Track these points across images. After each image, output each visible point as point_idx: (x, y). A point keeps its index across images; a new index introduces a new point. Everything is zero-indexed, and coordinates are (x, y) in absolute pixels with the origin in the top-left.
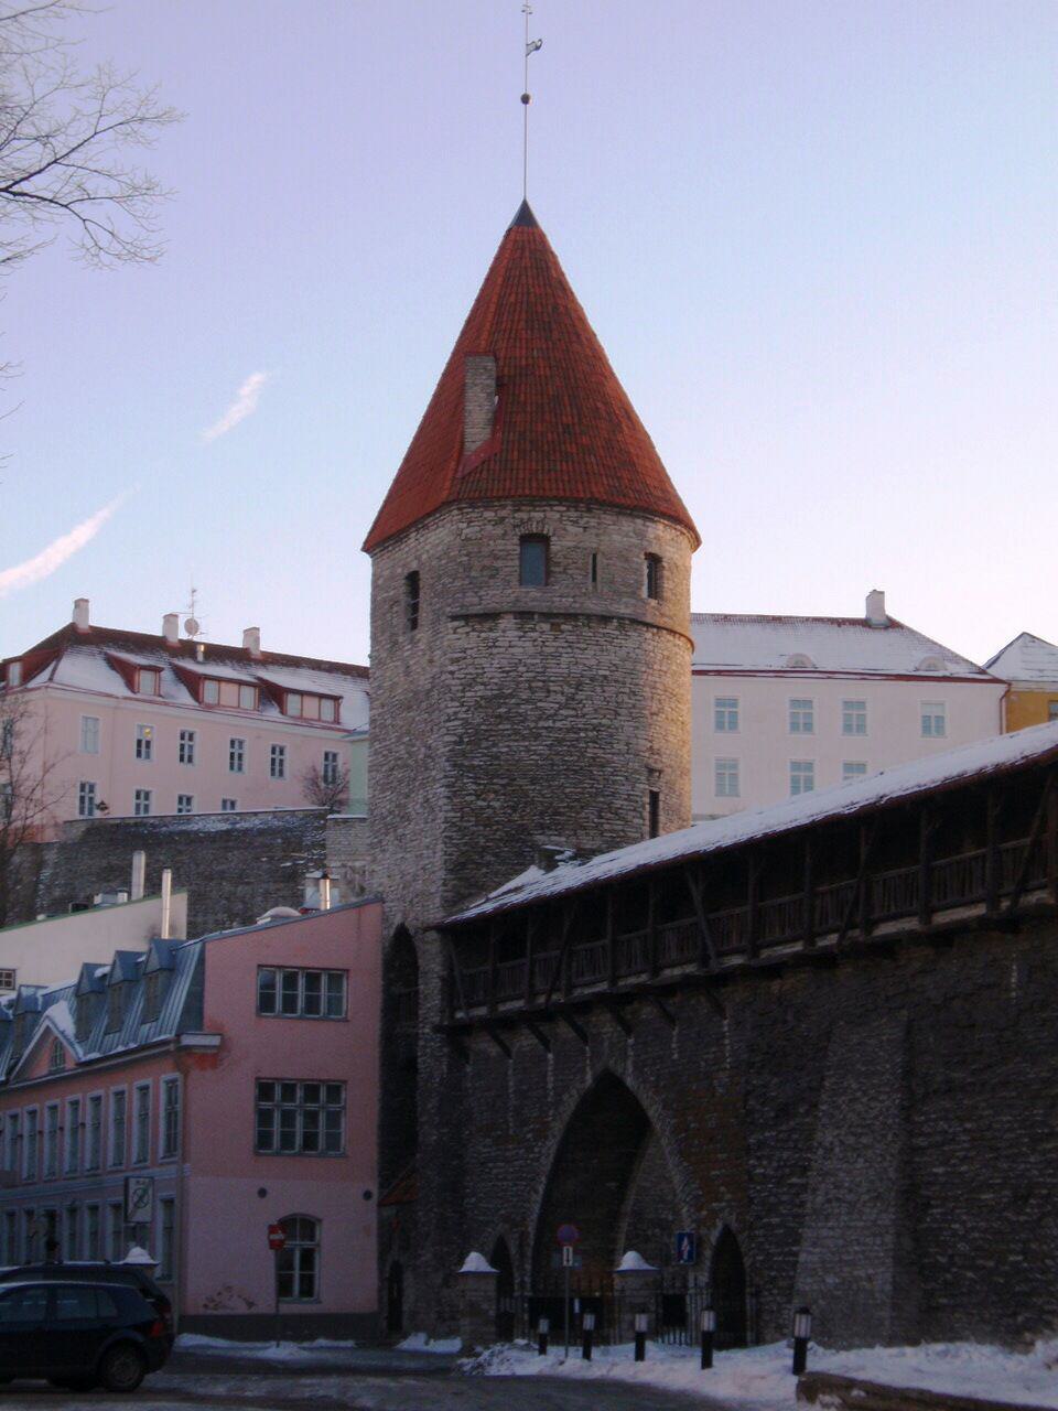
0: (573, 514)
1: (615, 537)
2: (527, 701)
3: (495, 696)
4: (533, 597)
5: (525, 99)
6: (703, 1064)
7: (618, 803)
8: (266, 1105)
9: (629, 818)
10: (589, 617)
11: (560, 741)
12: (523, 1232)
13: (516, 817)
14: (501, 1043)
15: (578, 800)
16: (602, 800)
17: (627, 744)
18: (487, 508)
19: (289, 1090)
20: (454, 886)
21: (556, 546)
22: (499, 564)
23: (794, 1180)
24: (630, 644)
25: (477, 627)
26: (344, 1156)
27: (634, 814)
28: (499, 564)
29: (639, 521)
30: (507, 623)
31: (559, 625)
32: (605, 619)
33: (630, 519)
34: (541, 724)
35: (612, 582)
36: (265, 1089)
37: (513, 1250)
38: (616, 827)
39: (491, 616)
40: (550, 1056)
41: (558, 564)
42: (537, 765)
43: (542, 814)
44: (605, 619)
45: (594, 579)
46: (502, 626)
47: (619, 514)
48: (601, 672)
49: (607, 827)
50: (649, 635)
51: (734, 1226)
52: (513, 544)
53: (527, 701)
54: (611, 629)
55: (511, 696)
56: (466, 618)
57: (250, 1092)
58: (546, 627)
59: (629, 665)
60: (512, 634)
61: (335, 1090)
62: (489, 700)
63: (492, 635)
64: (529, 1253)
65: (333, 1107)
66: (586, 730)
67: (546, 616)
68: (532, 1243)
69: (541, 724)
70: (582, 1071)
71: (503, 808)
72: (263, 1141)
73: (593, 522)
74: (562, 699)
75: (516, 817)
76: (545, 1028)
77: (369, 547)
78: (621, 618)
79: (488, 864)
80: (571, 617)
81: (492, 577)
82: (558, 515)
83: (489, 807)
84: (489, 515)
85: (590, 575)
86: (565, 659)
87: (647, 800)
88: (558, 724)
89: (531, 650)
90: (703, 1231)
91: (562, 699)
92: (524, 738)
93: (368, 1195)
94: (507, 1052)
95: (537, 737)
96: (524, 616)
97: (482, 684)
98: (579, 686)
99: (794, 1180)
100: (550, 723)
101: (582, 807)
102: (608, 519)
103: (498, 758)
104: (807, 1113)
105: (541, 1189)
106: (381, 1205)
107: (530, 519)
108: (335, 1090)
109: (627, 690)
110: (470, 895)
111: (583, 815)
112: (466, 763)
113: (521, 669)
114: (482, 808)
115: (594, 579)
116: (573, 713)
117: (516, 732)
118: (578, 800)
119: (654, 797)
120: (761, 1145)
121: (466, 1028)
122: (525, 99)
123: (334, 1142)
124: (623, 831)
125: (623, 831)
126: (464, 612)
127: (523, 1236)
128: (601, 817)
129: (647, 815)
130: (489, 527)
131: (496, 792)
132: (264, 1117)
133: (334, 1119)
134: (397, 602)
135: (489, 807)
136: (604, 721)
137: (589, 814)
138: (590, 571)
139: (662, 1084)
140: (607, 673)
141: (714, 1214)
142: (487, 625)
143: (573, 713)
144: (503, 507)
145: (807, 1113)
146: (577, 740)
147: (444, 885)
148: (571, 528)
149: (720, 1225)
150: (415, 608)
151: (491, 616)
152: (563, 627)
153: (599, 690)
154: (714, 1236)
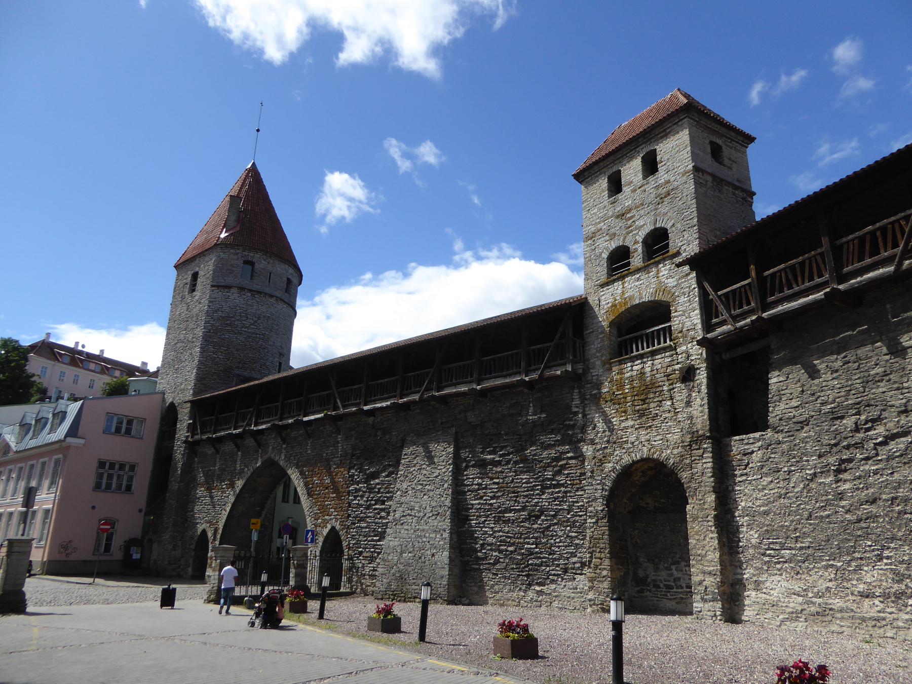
1: (278, 269)
2: (238, 320)
3: (226, 317)
4: (246, 283)
5: (258, 130)
6: (325, 455)
8: (101, 471)
10: (266, 294)
11: (249, 337)
12: (216, 528)
13: (228, 362)
14: (216, 449)
15: (253, 360)
18: (232, 248)
19: (112, 466)
20: (199, 387)
21: (257, 266)
22: (234, 269)
23: (377, 506)
25: (222, 290)
26: (133, 493)
28: (234, 269)
29: (287, 266)
30: (234, 290)
32: (271, 296)
36: (102, 464)
37: (210, 535)
39: (229, 287)
40: (239, 453)
41: (257, 273)
42: (239, 344)
43: (239, 363)
45: (269, 282)
46: (232, 292)
50: (285, 306)
51: (338, 527)
52: (240, 262)
53: (238, 320)
54: (273, 300)
55: (232, 317)
56: (218, 287)
57: (95, 464)
58: (249, 294)
60: (236, 295)
61: (132, 467)
62: (224, 317)
63: (228, 294)
64: (219, 536)
65: (131, 474)
66: (260, 334)
67: (250, 291)
68: (221, 532)
70: (257, 460)
71: (223, 358)
72: (98, 486)
73: (271, 261)
74: (252, 322)
75: (228, 362)
76: (239, 441)
77: (176, 267)
79: (215, 379)
80: (259, 293)
81: (230, 273)
82: (259, 256)
83: (218, 357)
84: (232, 251)
86: (255, 307)
87: (278, 364)
88: (249, 331)
89: (243, 302)
90: (318, 529)
91: (252, 322)
92: (236, 334)
93: (140, 511)
94: (217, 452)
95: (241, 334)
96: (242, 289)
97: (222, 311)
98: (259, 318)
99: (377, 506)
100: (246, 330)
103: (224, 340)
104: (387, 476)
105: (228, 509)
106: (145, 515)
107: (248, 255)
108: (132, 467)
110: (205, 390)
111: (254, 365)
112: (211, 340)
114: (215, 357)
115: (269, 282)
117: (232, 331)
118: (253, 360)
119: (280, 364)
120: (357, 490)
121: (198, 443)
123: (129, 488)
126: (217, 284)
127: (216, 530)
130: (232, 256)
131: (221, 352)
132: (100, 476)
133: (131, 479)
134: (186, 284)
135: (218, 357)
136: (267, 333)
139: (300, 464)
141: (326, 522)
142: (226, 290)
144: (239, 249)
145: (387, 476)
146: (256, 337)
147: (195, 386)
149: (329, 526)
150: (195, 285)
151: (229, 287)
154: (325, 531)
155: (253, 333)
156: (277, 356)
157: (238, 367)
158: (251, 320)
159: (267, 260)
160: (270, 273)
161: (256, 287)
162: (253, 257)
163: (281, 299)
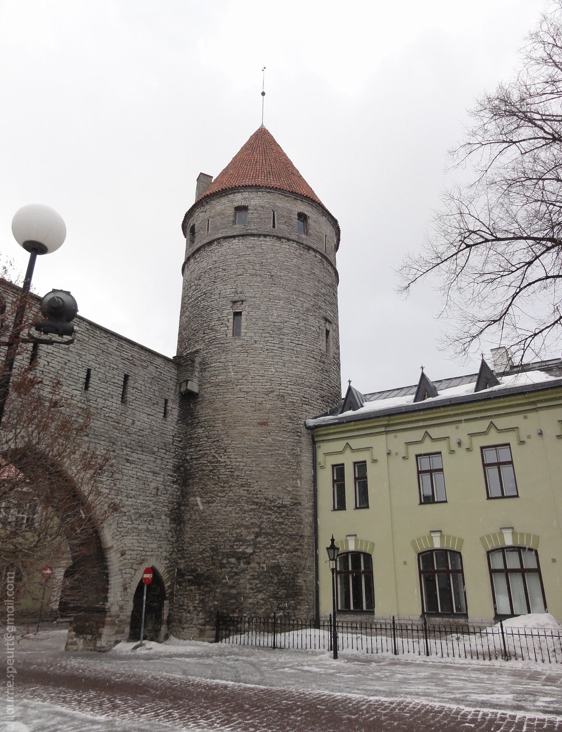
9: (218, 329)
16: (205, 325)
17: (219, 294)
24: (223, 249)
27: (222, 326)
33: (226, 197)
38: (211, 336)
48: (208, 268)
50: (233, 242)
54: (214, 246)
73: (208, 207)
74: (194, 287)
85: (207, 230)
101: (198, 332)
102: (214, 202)
124: (215, 336)
125: (215, 336)
128: (204, 333)
129: (230, 324)
153: (207, 276)
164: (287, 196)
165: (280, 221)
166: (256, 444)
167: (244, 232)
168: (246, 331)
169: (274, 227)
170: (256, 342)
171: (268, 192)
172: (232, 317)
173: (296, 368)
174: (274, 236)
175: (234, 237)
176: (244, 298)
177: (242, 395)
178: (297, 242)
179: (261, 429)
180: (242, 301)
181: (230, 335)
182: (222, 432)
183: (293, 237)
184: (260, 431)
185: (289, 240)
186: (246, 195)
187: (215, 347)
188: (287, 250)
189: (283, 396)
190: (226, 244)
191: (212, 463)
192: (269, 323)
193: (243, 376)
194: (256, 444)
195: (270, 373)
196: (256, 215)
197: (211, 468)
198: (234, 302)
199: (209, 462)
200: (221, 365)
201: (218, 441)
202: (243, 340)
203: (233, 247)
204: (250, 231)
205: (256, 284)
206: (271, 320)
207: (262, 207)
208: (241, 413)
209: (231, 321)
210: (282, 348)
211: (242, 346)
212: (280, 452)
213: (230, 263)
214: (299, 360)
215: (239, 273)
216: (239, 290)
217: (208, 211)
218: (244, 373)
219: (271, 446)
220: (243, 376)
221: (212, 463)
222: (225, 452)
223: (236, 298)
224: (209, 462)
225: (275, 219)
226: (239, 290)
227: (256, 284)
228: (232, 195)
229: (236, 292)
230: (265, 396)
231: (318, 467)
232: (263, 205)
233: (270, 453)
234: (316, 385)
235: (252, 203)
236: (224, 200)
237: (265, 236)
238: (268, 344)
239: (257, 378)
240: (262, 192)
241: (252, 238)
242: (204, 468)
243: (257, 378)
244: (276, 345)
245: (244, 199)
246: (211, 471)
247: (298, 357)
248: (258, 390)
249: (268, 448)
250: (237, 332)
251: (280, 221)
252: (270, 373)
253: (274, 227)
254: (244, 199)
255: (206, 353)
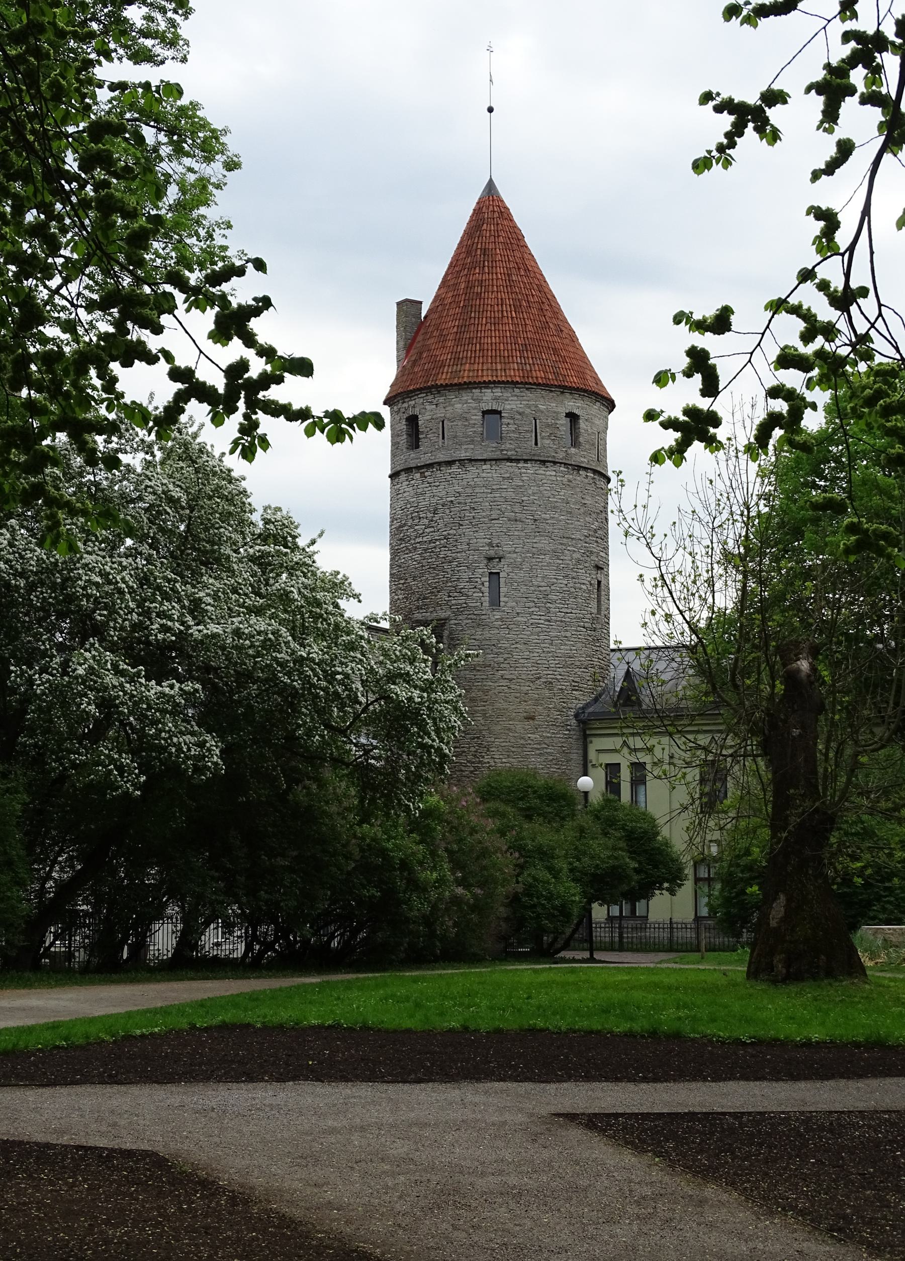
0: (430, 397)
1: (459, 406)
5: (490, 110)
7: (462, 585)
9: (470, 594)
10: (439, 464)
11: (425, 550)
24: (469, 476)
31: (424, 473)
32: (450, 463)
34: (418, 540)
35: (456, 437)
38: (460, 602)
44: (450, 463)
45: (443, 438)
47: (459, 389)
48: (449, 499)
49: (453, 602)
50: (484, 467)
54: (454, 469)
55: (405, 525)
58: (418, 475)
59: (469, 490)
67: (418, 468)
69: (418, 540)
73: (441, 400)
74: (426, 521)
78: (459, 460)
80: (429, 466)
82: (421, 400)
85: (441, 436)
88: (425, 539)
100: (420, 539)
101: (439, 592)
109: (468, 508)
113: (409, 506)
115: (443, 438)
116: (432, 529)
122: (490, 110)
128: (450, 596)
129: (486, 589)
137: (443, 595)
138: (441, 433)
140: (453, 499)
143: (432, 529)
148: (428, 407)
152: (426, 474)
153: (447, 511)
155: (430, 542)
156: (482, 566)
157: (418, 608)
158: (425, 520)
159: (435, 401)
160: (443, 422)
161: (426, 459)
162: (414, 407)
163: (470, 460)
164: (551, 391)
165: (543, 434)
166: (522, 742)
167: (497, 455)
168: (506, 599)
169: (536, 444)
170: (518, 613)
171: (527, 389)
172: (487, 579)
173: (566, 645)
174: (536, 461)
175: (485, 460)
176: (501, 553)
177: (504, 683)
178: (565, 464)
179: (528, 724)
180: (500, 558)
181: (486, 604)
182: (483, 728)
183: (560, 456)
184: (527, 727)
185: (555, 463)
186: (498, 392)
187: (467, 619)
188: (554, 478)
189: (551, 683)
190: (473, 469)
191: (473, 763)
192: (532, 588)
193: (505, 660)
194: (522, 742)
195: (536, 654)
196: (512, 427)
197: (472, 769)
198: (490, 559)
199: (468, 762)
200: (476, 643)
201: (478, 738)
202: (504, 611)
203: (484, 475)
204: (505, 452)
205: (516, 533)
206: (536, 583)
207: (520, 414)
208: (505, 705)
209: (487, 584)
210: (549, 621)
211: (501, 619)
212: (549, 750)
213: (481, 500)
214: (568, 634)
215: (493, 517)
216: (495, 541)
217: (442, 406)
218: (507, 656)
219: (540, 744)
220: (505, 660)
221: (473, 763)
222: (488, 750)
223: (492, 553)
224: (468, 762)
225: (538, 431)
226: (495, 541)
227: (516, 533)
228: (478, 391)
229: (490, 545)
230: (531, 684)
231: (590, 765)
232: (521, 410)
233: (538, 752)
234: (586, 663)
235: (508, 407)
236: (466, 396)
237: (526, 461)
238: (533, 617)
239: (521, 661)
240: (519, 388)
241: (509, 464)
242: (463, 768)
243: (521, 661)
244: (542, 617)
245: (496, 399)
246: (471, 772)
247: (567, 631)
248: (524, 677)
249: (535, 746)
250: (495, 602)
251: (543, 434)
252: (536, 654)
253: (536, 444)
254: (496, 399)
255: (455, 624)
